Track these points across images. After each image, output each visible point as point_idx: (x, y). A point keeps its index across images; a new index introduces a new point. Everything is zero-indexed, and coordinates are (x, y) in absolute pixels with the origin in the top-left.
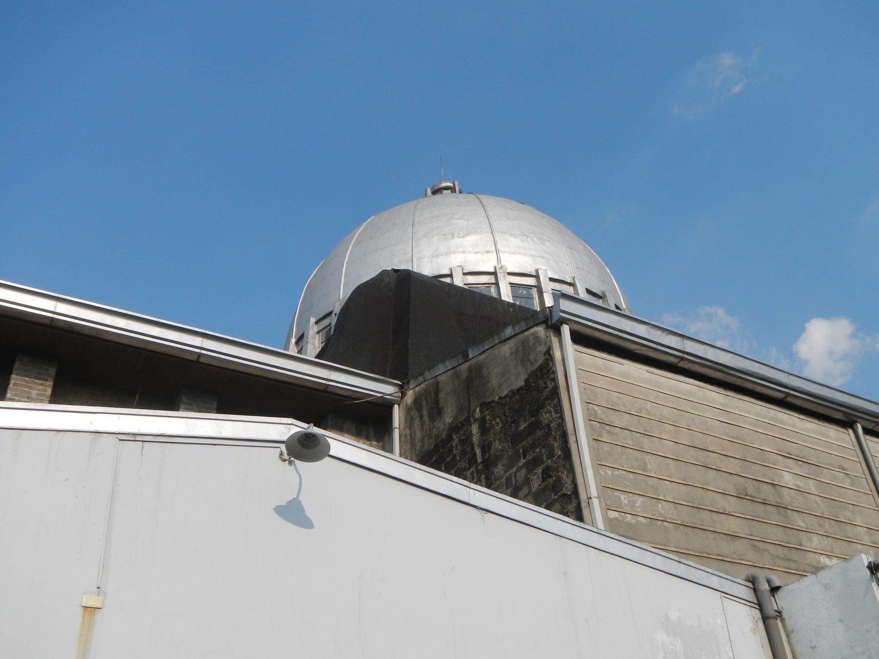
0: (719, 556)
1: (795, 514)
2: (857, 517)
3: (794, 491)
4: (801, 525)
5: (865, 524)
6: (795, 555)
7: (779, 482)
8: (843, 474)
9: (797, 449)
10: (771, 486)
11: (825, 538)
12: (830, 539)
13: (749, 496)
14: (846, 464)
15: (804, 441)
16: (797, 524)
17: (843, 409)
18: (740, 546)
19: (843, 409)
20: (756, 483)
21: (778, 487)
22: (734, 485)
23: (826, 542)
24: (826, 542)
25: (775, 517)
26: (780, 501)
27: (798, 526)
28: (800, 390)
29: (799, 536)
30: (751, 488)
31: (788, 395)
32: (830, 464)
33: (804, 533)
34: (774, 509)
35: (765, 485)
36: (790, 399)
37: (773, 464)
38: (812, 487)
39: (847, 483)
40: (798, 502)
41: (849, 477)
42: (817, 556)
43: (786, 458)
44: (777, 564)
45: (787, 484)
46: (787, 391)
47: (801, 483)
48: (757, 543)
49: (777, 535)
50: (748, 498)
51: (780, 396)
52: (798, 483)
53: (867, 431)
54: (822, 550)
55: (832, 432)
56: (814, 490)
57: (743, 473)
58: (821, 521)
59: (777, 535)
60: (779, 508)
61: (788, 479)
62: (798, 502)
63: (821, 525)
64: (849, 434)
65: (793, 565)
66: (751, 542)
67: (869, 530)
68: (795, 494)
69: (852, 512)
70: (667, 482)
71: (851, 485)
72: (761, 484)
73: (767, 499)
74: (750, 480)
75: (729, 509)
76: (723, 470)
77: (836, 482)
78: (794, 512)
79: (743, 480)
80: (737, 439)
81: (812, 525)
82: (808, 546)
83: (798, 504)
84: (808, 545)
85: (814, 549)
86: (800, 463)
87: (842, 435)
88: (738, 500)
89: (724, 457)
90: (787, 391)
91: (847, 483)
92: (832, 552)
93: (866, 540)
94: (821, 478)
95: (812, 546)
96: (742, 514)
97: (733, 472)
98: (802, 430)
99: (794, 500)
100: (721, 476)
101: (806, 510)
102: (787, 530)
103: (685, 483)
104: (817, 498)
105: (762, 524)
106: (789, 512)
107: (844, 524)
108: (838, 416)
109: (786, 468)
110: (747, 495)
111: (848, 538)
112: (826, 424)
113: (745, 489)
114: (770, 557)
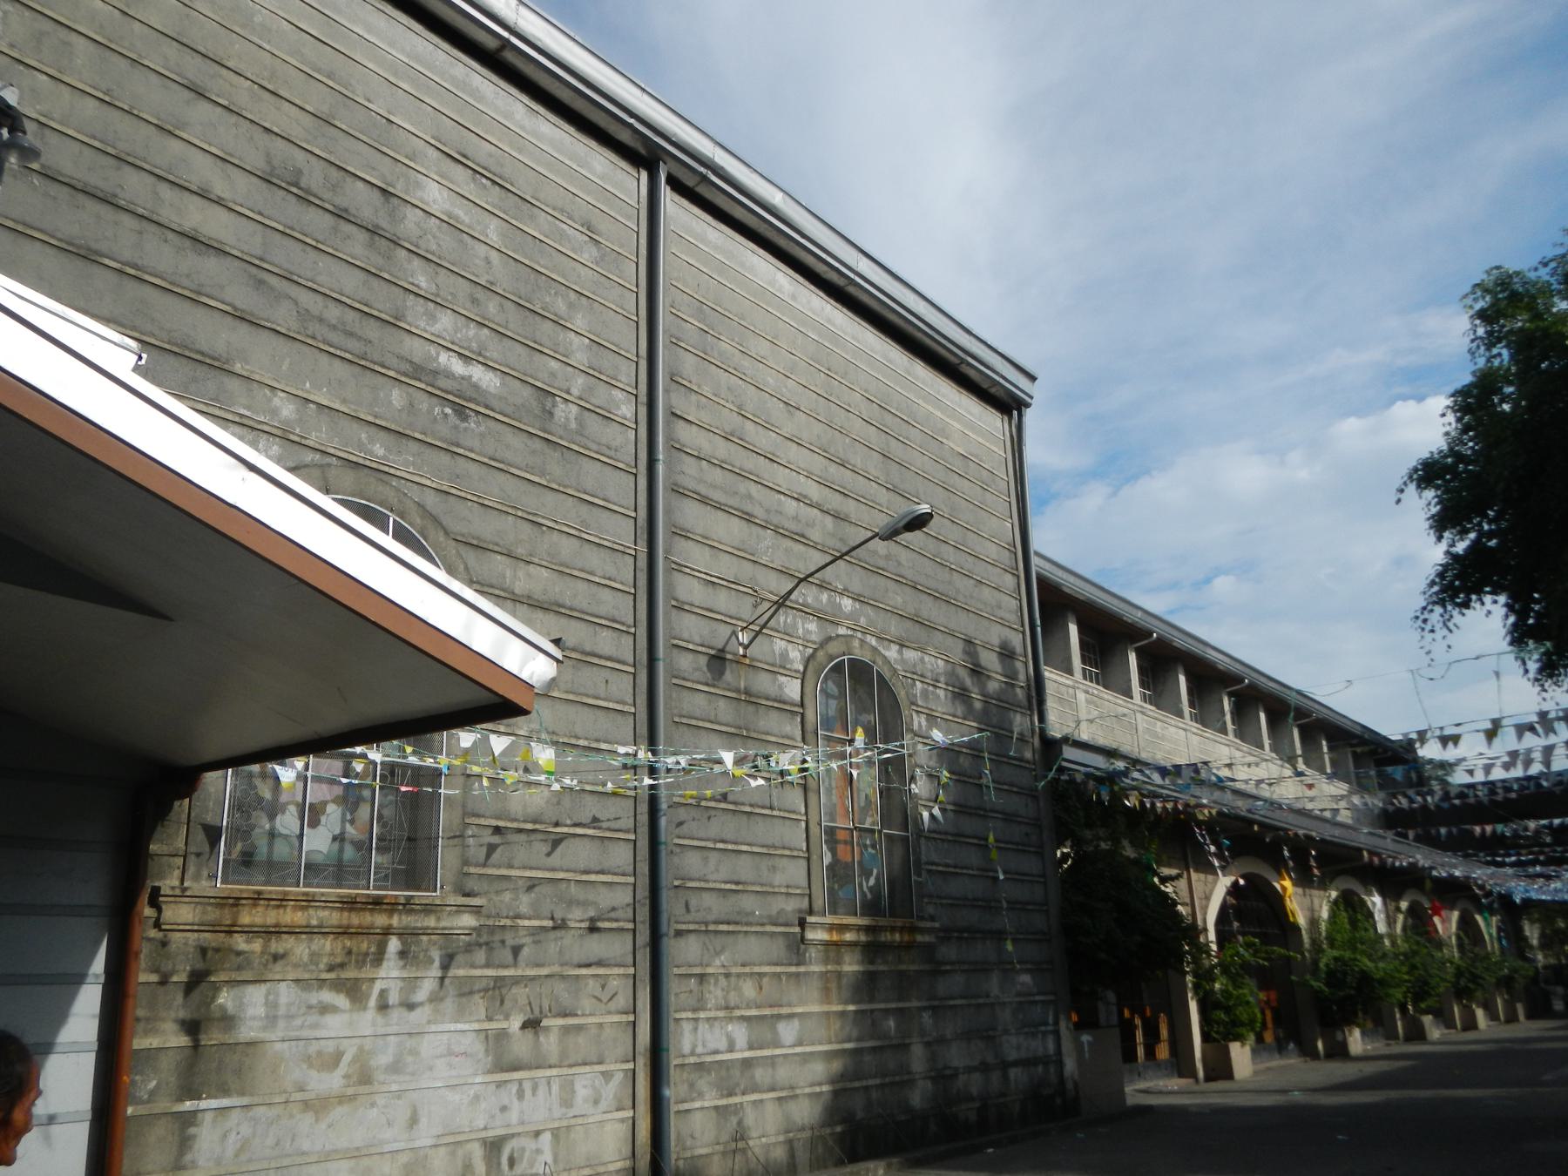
0: (133, 268)
1: (416, 262)
2: (580, 316)
3: (437, 221)
4: (423, 285)
5: (589, 332)
6: (372, 330)
7: (406, 193)
8: (588, 239)
9: (490, 155)
10: (376, 194)
11: (472, 325)
12: (486, 331)
13: (300, 188)
14: (603, 225)
15: (520, 151)
16: (411, 280)
17: (632, 121)
18: (211, 266)
19: (632, 121)
20: (334, 172)
21: (395, 201)
22: (268, 155)
23: (472, 331)
24: (471, 333)
25: (356, 245)
26: (384, 224)
27: (413, 284)
28: (539, 44)
29: (405, 301)
30: (315, 176)
31: (506, 44)
32: (562, 211)
33: (422, 301)
34: (362, 236)
35: (360, 184)
36: (509, 56)
37: (407, 157)
38: (493, 232)
39: (586, 256)
40: (440, 242)
41: (599, 249)
42: (433, 349)
43: (448, 160)
44: (309, 333)
45: (427, 204)
46: (505, 34)
47: (463, 214)
48: (274, 281)
49: (350, 283)
50: (295, 190)
51: (491, 44)
52: (461, 214)
53: (676, 185)
54: (453, 343)
55: (600, 163)
56: (493, 237)
57: (308, 142)
58: (480, 294)
59: (350, 283)
60: (377, 238)
61: (434, 195)
62: (439, 245)
63: (475, 301)
64: (638, 180)
65: (352, 344)
66: (254, 270)
67: (595, 344)
68: (439, 228)
69: (571, 306)
70: (45, 77)
71: (597, 264)
72: (349, 179)
73: (353, 211)
74: (322, 162)
75: (219, 189)
76: (249, 117)
77: (561, 244)
78: (414, 256)
79: (300, 156)
80: (329, 77)
81: (452, 294)
82: (422, 325)
83: (434, 247)
84: (422, 324)
85: (432, 334)
86: (484, 181)
87: (620, 175)
88: (264, 185)
89: (267, 95)
90: (505, 34)
91: (586, 256)
92: (480, 354)
93: (580, 358)
94: (525, 224)
95: (428, 328)
96: (260, 214)
97: (275, 129)
98: (523, 128)
99: (429, 237)
100: (236, 125)
101: (453, 264)
102: (375, 282)
103: (107, 99)
104: (494, 255)
105: (309, 249)
106: (404, 253)
107: (537, 318)
108: (624, 136)
109: (442, 176)
110: (296, 185)
111: (535, 342)
112: (593, 144)
113: (299, 172)
114: (295, 313)
